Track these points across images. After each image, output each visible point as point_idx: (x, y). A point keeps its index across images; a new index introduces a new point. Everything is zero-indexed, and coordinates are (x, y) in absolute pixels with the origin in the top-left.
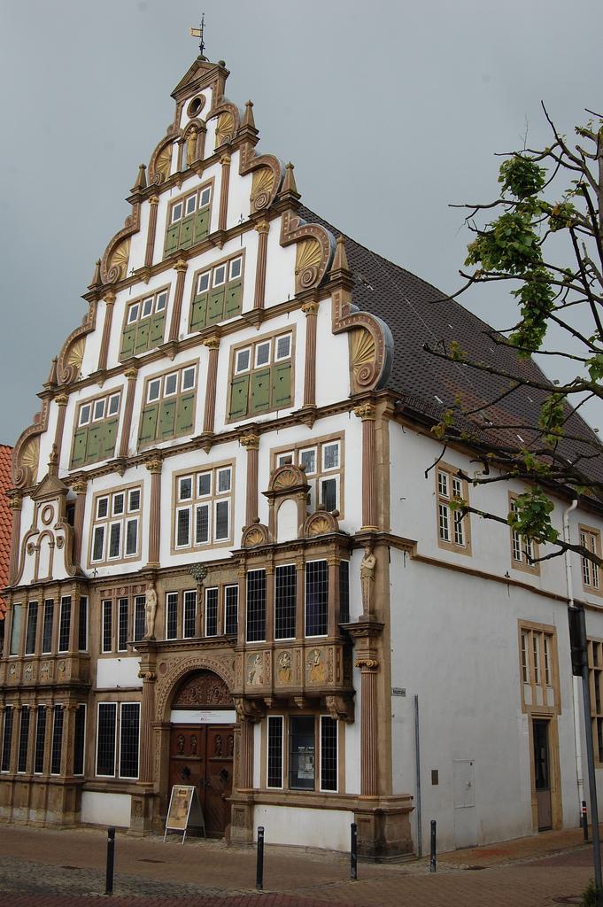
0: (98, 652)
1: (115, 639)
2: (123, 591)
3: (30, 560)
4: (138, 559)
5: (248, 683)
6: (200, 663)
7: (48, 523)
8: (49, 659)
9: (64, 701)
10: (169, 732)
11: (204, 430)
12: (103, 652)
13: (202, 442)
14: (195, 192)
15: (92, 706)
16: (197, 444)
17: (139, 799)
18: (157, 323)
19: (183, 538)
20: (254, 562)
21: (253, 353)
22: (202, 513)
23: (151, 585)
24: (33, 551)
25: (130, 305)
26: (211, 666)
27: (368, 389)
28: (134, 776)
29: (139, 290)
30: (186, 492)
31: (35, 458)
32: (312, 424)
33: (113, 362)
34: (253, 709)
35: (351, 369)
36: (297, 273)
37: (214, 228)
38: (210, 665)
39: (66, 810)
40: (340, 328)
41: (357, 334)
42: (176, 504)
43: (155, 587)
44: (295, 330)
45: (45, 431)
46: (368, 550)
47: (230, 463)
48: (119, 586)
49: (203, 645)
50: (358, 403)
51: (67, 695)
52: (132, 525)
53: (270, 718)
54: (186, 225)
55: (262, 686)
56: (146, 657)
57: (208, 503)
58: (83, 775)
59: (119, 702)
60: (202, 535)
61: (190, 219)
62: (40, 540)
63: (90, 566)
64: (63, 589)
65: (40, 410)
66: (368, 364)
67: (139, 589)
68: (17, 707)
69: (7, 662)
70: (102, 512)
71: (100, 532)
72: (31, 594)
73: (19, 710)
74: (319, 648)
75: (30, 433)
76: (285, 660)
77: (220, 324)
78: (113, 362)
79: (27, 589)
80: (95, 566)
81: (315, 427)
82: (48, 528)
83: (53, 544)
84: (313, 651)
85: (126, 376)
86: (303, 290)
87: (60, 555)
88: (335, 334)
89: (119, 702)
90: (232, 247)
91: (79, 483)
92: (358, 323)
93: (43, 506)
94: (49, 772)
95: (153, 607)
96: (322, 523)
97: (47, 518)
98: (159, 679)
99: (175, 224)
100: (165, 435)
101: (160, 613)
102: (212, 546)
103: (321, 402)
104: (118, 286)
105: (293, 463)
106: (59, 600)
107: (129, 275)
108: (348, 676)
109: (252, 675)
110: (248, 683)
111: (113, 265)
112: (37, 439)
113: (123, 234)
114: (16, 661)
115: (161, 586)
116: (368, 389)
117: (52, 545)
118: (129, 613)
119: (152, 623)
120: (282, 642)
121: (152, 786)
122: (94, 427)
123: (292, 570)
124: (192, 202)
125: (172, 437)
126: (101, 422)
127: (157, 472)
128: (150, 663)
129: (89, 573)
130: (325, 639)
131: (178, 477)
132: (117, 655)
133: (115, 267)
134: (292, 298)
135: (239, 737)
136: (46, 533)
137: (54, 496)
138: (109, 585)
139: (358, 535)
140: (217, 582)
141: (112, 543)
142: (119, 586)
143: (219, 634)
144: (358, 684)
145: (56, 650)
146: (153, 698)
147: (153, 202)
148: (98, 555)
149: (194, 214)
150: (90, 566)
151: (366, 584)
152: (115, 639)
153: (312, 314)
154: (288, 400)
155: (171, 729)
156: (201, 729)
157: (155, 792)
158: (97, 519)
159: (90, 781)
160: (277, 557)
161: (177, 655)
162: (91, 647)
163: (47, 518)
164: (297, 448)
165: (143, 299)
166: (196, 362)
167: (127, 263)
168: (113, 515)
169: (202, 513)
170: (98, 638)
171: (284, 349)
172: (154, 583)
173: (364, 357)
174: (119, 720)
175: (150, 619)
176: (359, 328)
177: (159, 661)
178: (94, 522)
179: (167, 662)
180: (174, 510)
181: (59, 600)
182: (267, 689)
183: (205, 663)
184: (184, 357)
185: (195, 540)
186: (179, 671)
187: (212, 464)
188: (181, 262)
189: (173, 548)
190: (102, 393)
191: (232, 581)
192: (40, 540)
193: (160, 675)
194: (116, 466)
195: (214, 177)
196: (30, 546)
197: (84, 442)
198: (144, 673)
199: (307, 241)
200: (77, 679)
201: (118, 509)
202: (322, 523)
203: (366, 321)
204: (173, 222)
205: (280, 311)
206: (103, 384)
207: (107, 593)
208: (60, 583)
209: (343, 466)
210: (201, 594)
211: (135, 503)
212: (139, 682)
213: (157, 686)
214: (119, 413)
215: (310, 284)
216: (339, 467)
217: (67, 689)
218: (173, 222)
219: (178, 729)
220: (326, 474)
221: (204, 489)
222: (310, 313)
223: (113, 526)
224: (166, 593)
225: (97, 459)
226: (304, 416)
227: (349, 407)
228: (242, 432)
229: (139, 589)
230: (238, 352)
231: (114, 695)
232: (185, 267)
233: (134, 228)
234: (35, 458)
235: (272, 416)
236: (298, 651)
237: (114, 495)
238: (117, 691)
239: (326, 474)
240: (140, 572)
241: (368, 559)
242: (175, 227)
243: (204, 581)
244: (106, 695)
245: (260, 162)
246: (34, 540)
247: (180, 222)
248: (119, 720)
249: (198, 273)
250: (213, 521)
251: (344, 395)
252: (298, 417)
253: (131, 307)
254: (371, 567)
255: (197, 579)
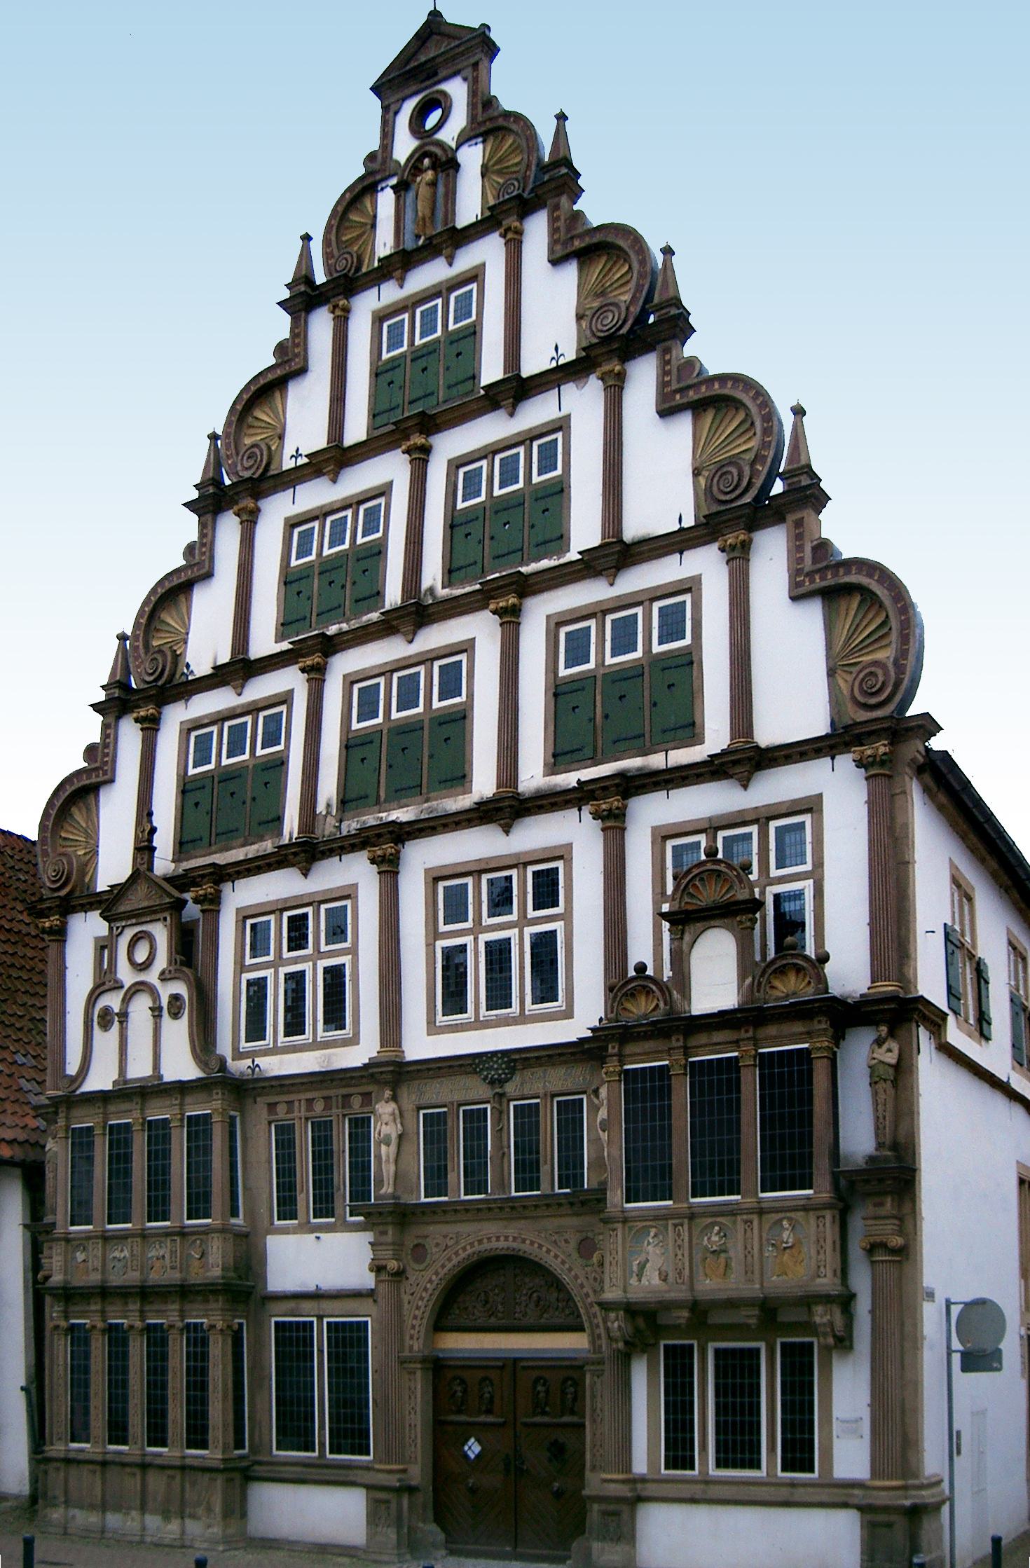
0: (266, 1222)
1: (306, 1197)
2: (319, 1107)
3: (105, 1042)
4: (354, 1040)
5: (633, 1281)
6: (502, 1244)
7: (146, 966)
8: (167, 1235)
9: (209, 1316)
10: (430, 1373)
11: (498, 788)
12: (277, 1222)
13: (499, 809)
14: (437, 294)
15: (258, 1325)
16: (484, 814)
17: (382, 1495)
18: (364, 564)
19: (455, 997)
20: (638, 1051)
21: (600, 637)
22: (498, 955)
23: (388, 1093)
24: (111, 1023)
25: (294, 526)
26: (526, 1248)
27: (879, 713)
28: (361, 1453)
29: (314, 495)
30: (456, 910)
31: (88, 836)
32: (749, 780)
33: (264, 642)
34: (637, 1330)
35: (831, 673)
36: (696, 473)
37: (491, 370)
38: (526, 1247)
39: (227, 1514)
40: (808, 586)
41: (843, 604)
42: (433, 934)
43: (394, 1098)
44: (700, 589)
45: (112, 781)
46: (884, 1029)
47: (563, 854)
48: (309, 1095)
49: (510, 1210)
50: (859, 740)
51: (217, 1305)
52: (335, 978)
53: (665, 1346)
54: (422, 363)
55: (664, 1286)
56: (384, 1233)
57: (513, 933)
58: (246, 1451)
59: (320, 1318)
60: (499, 995)
61: (429, 351)
62: (127, 1000)
63: (238, 1055)
64: (188, 1099)
65: (97, 738)
66: (875, 663)
67: (356, 1102)
68: (100, 1325)
69: (68, 1240)
70: (259, 947)
71: (257, 990)
72: (112, 1108)
73: (103, 1331)
74: (792, 1215)
75: (77, 784)
76: (715, 1238)
77: (524, 569)
78: (264, 642)
79: (102, 1097)
80: (252, 1054)
81: (751, 789)
82: (142, 977)
83: (160, 1009)
84: (781, 1220)
85: (303, 670)
86: (716, 508)
87: (177, 1033)
88: (794, 598)
89: (320, 1318)
90: (537, 412)
91: (208, 888)
92: (847, 579)
93: (129, 934)
94: (182, 1447)
95: (394, 1136)
96: (792, 977)
97: (141, 955)
98: (409, 1273)
99: (393, 359)
100: (399, 795)
101: (408, 1148)
102: (523, 1019)
103: (768, 733)
104: (266, 485)
105: (720, 856)
106: (182, 1120)
107: (288, 464)
108: (844, 1272)
109: (642, 1267)
110: (633, 1281)
111: (248, 441)
112: (92, 798)
113: (270, 377)
114: (89, 1238)
115: (409, 1097)
116: (879, 713)
117: (156, 1011)
118: (335, 1148)
119: (392, 1168)
120: (700, 1205)
121: (404, 1471)
122: (228, 776)
123: (731, 1066)
124: (429, 316)
125: (419, 798)
126: (241, 767)
127: (389, 868)
128: (393, 1244)
129: (239, 1067)
130: (808, 1198)
131: (437, 880)
132: (308, 1228)
133: (254, 445)
134: (689, 522)
135: (597, 1388)
136: (139, 987)
137: (155, 912)
138: (289, 1092)
139: (865, 1001)
140: (538, 1087)
141: (287, 1009)
142: (309, 1095)
143: (545, 1188)
144: (861, 1282)
145: (180, 1216)
146: (400, 1315)
147: (338, 312)
148: (256, 1029)
149: (437, 341)
150: (238, 1055)
151: (882, 1096)
152: (306, 1197)
153: (739, 558)
154: (691, 731)
155: (438, 1367)
156: (502, 1368)
157: (413, 1483)
158: (248, 961)
159: (260, 1463)
160: (693, 1042)
161: (451, 1229)
162: (251, 1215)
163: (141, 956)
164: (711, 827)
165: (326, 514)
166: (467, 647)
167: (281, 437)
168: (286, 955)
169: (498, 955)
170: (265, 1196)
171: (672, 625)
172: (394, 1090)
173: (862, 648)
174: (321, 1351)
175: (388, 1161)
176: (850, 589)
177: (410, 1242)
178: (241, 967)
179: (429, 1244)
180: (430, 946)
181: (182, 1120)
182: (680, 1293)
183: (515, 1245)
184: (436, 637)
185: (528, 998)
186: (455, 1261)
187: (517, 855)
188: (418, 440)
189: (431, 1021)
190: (243, 705)
191: (570, 1086)
192: (127, 1000)
193: (412, 1266)
194: (295, 854)
195: (484, 265)
196: (106, 1012)
197: (205, 806)
198: (383, 1262)
199: (718, 410)
200: (232, 1274)
201: (298, 938)
202: (792, 977)
203: (870, 576)
204: (385, 356)
205: (656, 549)
206: (243, 686)
207: (282, 1109)
208: (182, 1088)
209: (819, 864)
210: (501, 1112)
211: (337, 931)
212: (367, 1280)
213: (406, 1287)
214: (287, 746)
215: (733, 496)
216: (808, 867)
217: (215, 1292)
218: (385, 356)
219: (450, 1367)
220: (782, 880)
221: (501, 900)
222: (736, 554)
223: (327, 970)
224: (419, 1108)
225: (241, 840)
226: (735, 763)
227: (832, 747)
228: (593, 791)
229: (356, 1102)
230: (563, 631)
231: (307, 1306)
232: (426, 450)
233: (295, 366)
234: (88, 836)
235: (657, 761)
236: (746, 1222)
237: (286, 914)
238: (317, 1296)
239: (782, 880)
240: (366, 1066)
241: (885, 1047)
242: (394, 364)
243: (510, 1088)
244: (291, 1304)
245: (597, 238)
246: (113, 1001)
247: (403, 355)
248: (321, 1351)
249: (455, 465)
250: (522, 968)
251: (817, 725)
252: (722, 764)
253: (296, 531)
254: (894, 1061)
255: (492, 1083)
